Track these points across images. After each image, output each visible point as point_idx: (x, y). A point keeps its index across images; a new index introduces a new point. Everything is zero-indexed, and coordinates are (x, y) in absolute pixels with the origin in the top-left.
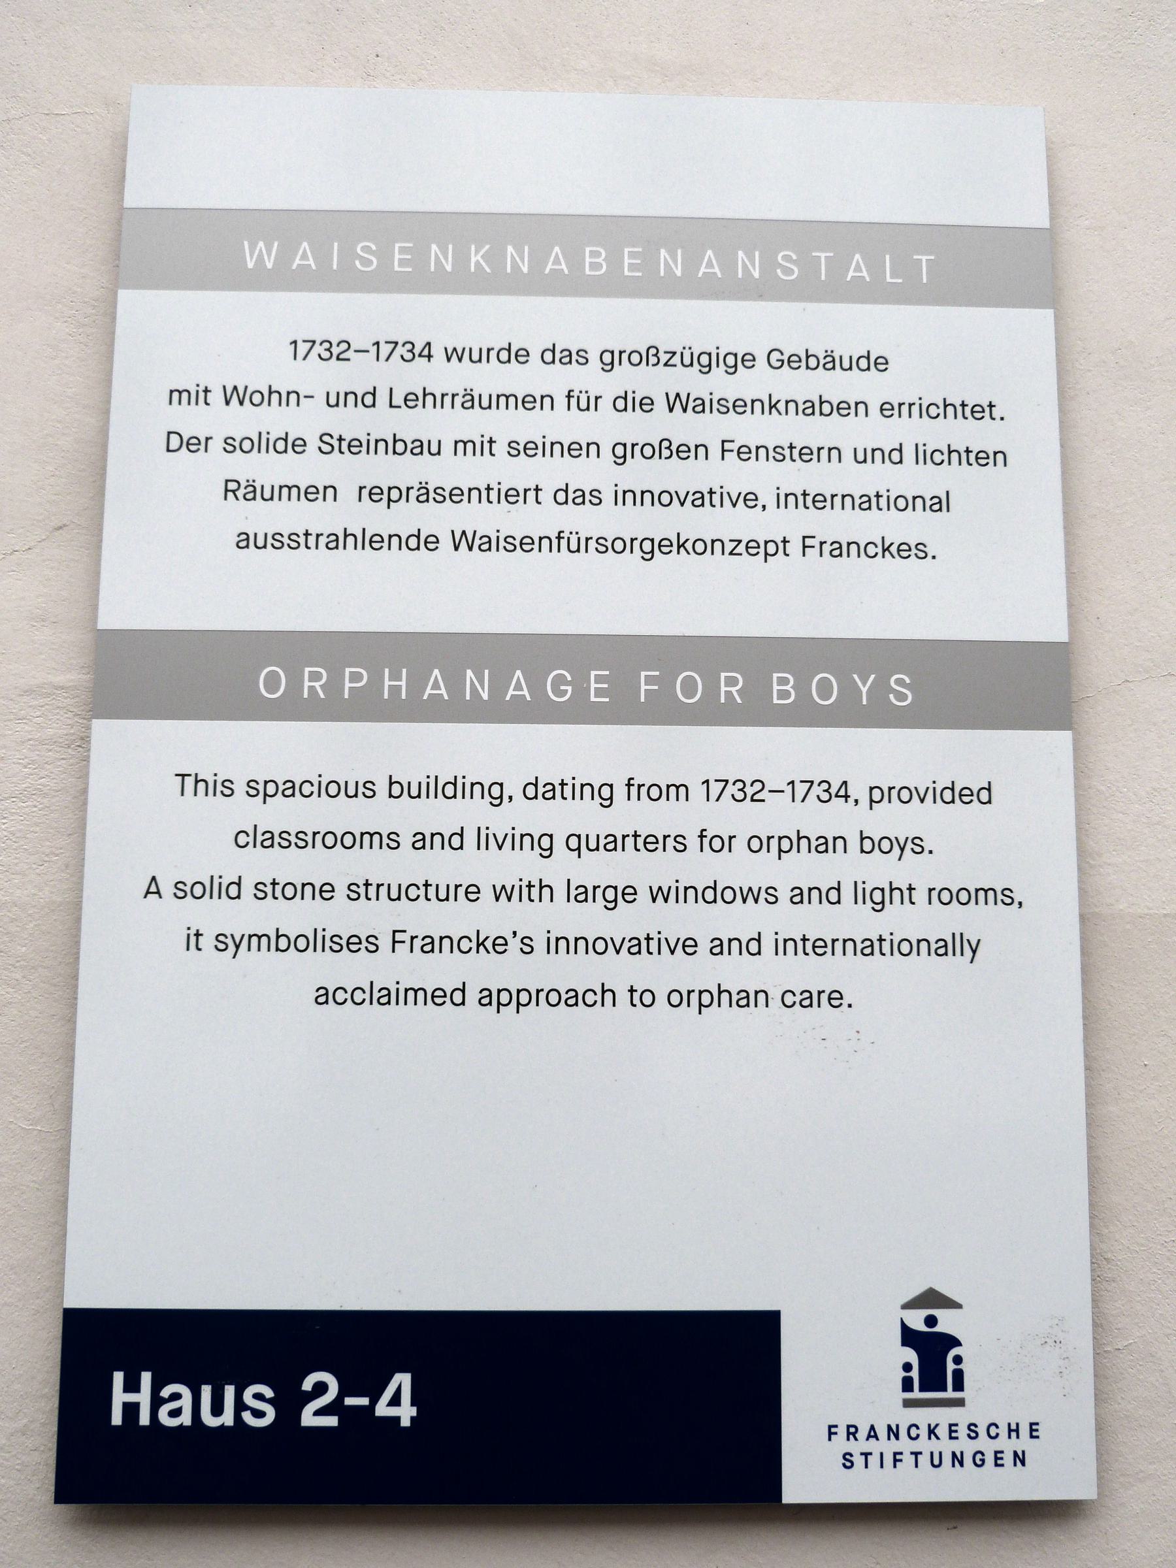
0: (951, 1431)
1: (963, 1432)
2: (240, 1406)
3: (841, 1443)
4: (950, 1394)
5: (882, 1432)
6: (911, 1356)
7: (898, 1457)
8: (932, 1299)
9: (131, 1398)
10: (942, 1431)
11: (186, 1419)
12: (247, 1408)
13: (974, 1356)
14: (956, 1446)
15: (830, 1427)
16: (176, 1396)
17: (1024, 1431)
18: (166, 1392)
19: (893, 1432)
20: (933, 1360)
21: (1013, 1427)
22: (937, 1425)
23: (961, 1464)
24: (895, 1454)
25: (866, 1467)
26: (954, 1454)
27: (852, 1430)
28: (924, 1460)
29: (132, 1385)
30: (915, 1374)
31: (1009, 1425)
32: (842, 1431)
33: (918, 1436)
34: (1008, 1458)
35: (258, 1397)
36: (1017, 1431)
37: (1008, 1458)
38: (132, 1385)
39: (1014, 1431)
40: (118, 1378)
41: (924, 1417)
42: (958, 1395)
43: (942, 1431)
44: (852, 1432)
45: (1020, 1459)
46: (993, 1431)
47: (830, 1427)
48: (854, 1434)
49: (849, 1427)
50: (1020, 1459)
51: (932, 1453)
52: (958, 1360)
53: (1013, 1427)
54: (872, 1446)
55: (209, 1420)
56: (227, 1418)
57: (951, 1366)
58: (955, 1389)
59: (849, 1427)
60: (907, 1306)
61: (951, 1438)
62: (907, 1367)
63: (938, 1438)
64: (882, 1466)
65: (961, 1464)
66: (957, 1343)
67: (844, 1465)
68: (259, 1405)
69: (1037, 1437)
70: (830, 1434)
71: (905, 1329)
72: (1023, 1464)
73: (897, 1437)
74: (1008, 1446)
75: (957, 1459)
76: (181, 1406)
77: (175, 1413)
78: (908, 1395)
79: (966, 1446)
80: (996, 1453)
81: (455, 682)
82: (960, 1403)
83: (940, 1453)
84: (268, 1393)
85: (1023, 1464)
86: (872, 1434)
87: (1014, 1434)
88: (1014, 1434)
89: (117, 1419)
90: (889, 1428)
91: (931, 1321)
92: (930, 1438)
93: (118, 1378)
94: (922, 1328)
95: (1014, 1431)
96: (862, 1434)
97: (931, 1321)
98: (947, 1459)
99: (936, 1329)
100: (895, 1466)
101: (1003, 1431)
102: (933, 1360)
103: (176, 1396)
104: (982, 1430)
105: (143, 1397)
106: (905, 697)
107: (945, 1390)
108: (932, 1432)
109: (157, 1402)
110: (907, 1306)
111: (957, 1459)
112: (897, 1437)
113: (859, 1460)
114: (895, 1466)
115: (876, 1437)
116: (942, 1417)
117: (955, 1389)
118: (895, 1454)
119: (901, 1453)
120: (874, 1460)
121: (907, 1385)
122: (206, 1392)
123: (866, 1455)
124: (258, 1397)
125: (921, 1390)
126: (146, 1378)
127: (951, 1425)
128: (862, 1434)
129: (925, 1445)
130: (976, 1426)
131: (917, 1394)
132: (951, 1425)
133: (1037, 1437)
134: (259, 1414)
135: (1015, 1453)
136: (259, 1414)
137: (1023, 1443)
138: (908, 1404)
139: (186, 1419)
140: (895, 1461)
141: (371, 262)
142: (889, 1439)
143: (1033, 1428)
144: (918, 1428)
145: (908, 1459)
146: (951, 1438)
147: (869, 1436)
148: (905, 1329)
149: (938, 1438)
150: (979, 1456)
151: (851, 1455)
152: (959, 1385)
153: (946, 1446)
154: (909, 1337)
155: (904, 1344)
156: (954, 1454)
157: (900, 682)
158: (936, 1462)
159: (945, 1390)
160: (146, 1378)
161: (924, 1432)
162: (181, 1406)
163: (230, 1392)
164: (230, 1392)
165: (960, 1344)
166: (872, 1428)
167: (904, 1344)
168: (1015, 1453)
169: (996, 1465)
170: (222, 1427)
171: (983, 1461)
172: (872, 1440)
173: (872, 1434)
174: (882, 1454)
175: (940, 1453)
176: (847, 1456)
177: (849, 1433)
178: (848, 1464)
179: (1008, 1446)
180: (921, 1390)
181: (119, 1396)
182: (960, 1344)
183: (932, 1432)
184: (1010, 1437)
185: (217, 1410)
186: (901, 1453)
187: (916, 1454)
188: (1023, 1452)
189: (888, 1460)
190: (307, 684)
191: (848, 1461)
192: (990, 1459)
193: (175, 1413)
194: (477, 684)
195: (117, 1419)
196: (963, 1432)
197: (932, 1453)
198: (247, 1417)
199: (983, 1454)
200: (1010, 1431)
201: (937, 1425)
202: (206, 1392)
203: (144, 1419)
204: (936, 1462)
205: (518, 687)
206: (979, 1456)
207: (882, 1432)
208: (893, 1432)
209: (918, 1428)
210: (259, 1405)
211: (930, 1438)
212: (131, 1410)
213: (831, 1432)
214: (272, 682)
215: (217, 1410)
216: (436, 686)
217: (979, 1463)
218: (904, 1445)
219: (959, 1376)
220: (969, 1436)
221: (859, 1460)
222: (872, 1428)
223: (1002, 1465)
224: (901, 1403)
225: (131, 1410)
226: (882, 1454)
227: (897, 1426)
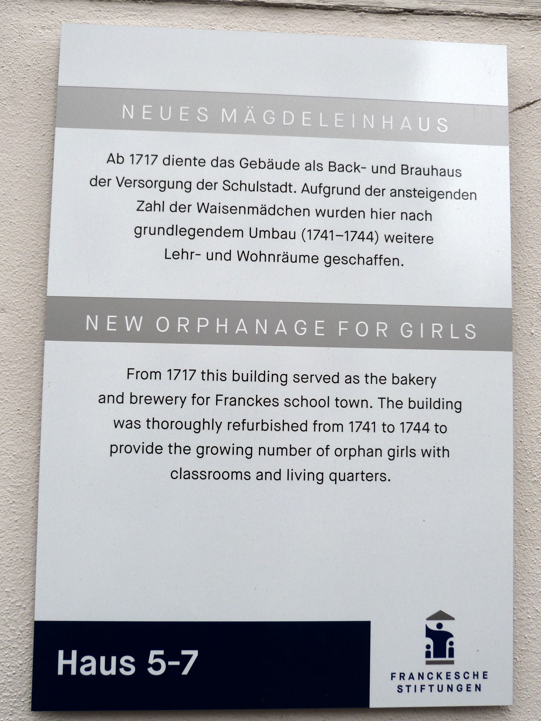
0: (447, 676)
1: (452, 676)
2: (119, 666)
3: (397, 681)
4: (447, 658)
5: (416, 676)
6: (430, 642)
7: (423, 687)
8: (441, 615)
9: (67, 662)
10: (443, 676)
11: (93, 672)
12: (122, 666)
14: (449, 682)
16: (88, 661)
17: (481, 675)
18: (83, 660)
19: (421, 676)
20: (440, 643)
21: (476, 673)
22: (441, 673)
23: (452, 690)
24: (421, 686)
25: (408, 691)
26: (448, 686)
27: (402, 675)
28: (435, 688)
29: (67, 656)
30: (431, 650)
31: (474, 673)
32: (398, 676)
34: (473, 688)
35: (127, 661)
36: (477, 675)
37: (473, 688)
38: (67, 656)
39: (476, 675)
40: (61, 653)
42: (451, 659)
43: (443, 676)
44: (402, 676)
45: (478, 688)
47: (392, 674)
48: (403, 677)
49: (401, 674)
50: (478, 688)
51: (438, 686)
52: (451, 643)
53: (476, 673)
54: (411, 682)
57: (448, 646)
60: (428, 619)
61: (447, 678)
62: (428, 647)
63: (441, 679)
64: (415, 691)
65: (452, 690)
66: (451, 636)
67: (398, 691)
68: (127, 665)
69: (486, 678)
70: (392, 677)
71: (427, 628)
72: (480, 690)
73: (423, 678)
74: (473, 682)
75: (450, 688)
76: (91, 666)
77: (88, 669)
78: (428, 659)
79: (454, 682)
80: (467, 685)
81: (251, 326)
82: (452, 663)
83: (442, 686)
84: (132, 660)
85: (480, 690)
86: (411, 677)
87: (476, 677)
88: (476, 677)
89: (60, 672)
90: (419, 674)
91: (440, 626)
92: (437, 679)
93: (61, 653)
95: (476, 675)
97: (440, 626)
98: (445, 688)
99: (442, 629)
100: (421, 691)
101: (471, 675)
102: (440, 643)
103: (88, 661)
104: (461, 675)
105: (73, 662)
106: (472, 335)
107: (445, 657)
108: (438, 676)
109: (79, 664)
110: (428, 619)
111: (450, 688)
112: (423, 678)
113: (405, 689)
114: (421, 691)
115: (413, 678)
116: (443, 669)
119: (424, 686)
120: (412, 689)
121: (428, 655)
122: (103, 659)
123: (408, 686)
124: (127, 661)
125: (434, 657)
126: (74, 653)
127: (447, 673)
129: (435, 682)
130: (459, 673)
131: (432, 659)
132: (447, 673)
134: (128, 669)
135: (476, 686)
136: (128, 669)
137: (480, 681)
138: (428, 663)
139: (93, 672)
140: (422, 689)
141: (426, 128)
142: (419, 679)
143: (485, 674)
144: (432, 674)
145: (428, 688)
146: (447, 678)
147: (410, 678)
148: (427, 628)
149: (441, 679)
150: (460, 687)
151: (401, 686)
152: (451, 655)
153: (445, 682)
154: (429, 633)
155: (427, 636)
156: (448, 686)
157: (470, 328)
158: (440, 689)
159: (445, 657)
160: (74, 653)
161: (435, 676)
162: (91, 666)
163: (114, 659)
164: (114, 659)
166: (411, 674)
167: (427, 636)
168: (476, 686)
169: (467, 690)
170: (110, 675)
171: (461, 689)
172: (411, 680)
173: (411, 677)
174: (415, 686)
175: (442, 686)
177: (401, 676)
178: (400, 690)
179: (473, 682)
180: (434, 657)
181: (61, 662)
182: (451, 636)
183: (438, 676)
184: (474, 678)
185: (108, 667)
186: (424, 686)
187: (431, 686)
188: (480, 685)
189: (418, 689)
190: (179, 325)
191: (400, 689)
192: (464, 688)
193: (88, 669)
194: (261, 326)
195: (60, 672)
196: (452, 676)
197: (438, 686)
198: (122, 671)
199: (461, 686)
200: (474, 675)
201: (441, 673)
202: (103, 659)
203: (74, 672)
204: (440, 689)
205: (281, 328)
206: (460, 687)
207: (416, 676)
208: (421, 676)
209: (432, 674)
210: (127, 665)
211: (437, 679)
212: (67, 668)
213: (393, 676)
214: (163, 324)
215: (108, 667)
216: (242, 327)
217: (459, 689)
218: (426, 682)
219: (452, 651)
220: (455, 678)
221: (405, 689)
222: (411, 674)
223: (470, 691)
224: (425, 662)
225: (67, 668)
226: (415, 686)
227: (423, 673)
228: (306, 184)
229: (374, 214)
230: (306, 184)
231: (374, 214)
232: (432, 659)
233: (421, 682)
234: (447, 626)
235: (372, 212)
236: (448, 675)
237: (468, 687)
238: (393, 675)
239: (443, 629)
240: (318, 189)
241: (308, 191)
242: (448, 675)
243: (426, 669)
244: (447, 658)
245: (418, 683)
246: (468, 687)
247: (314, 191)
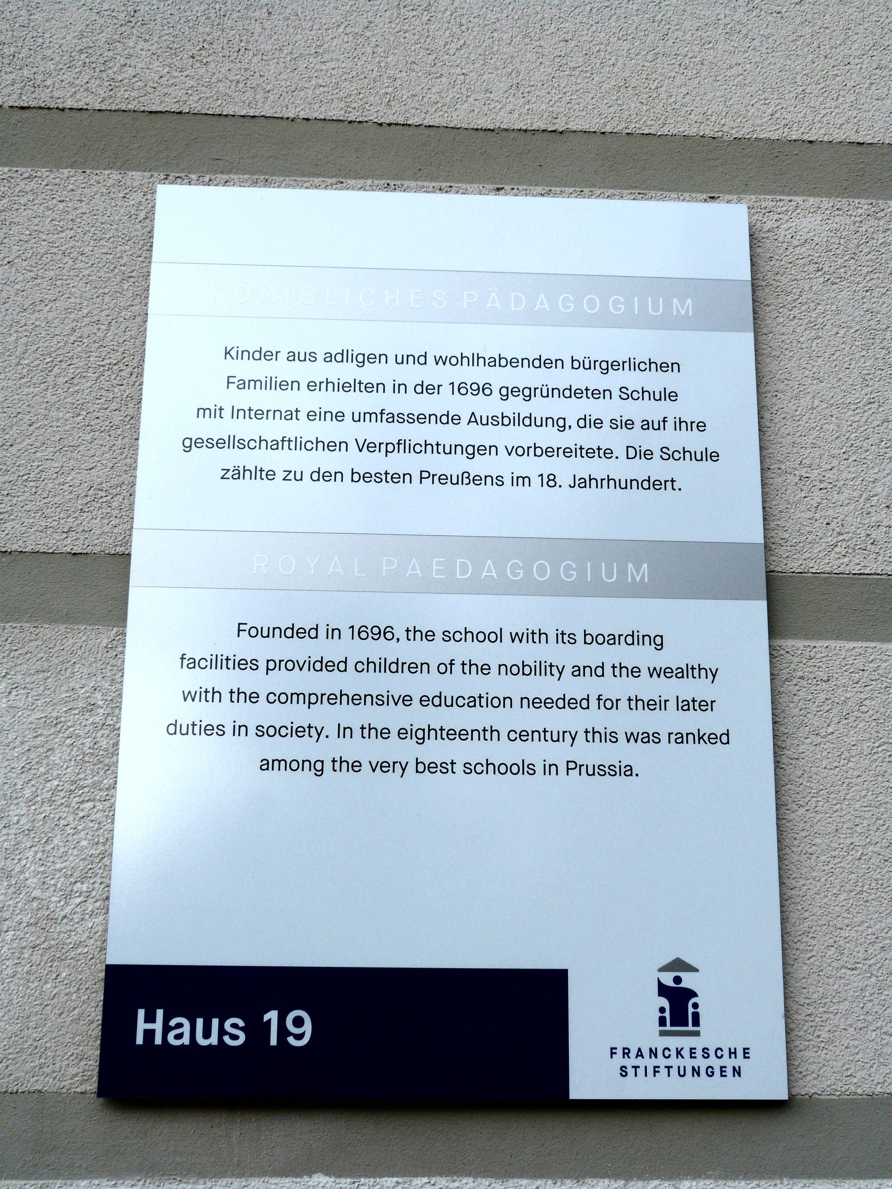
0: (691, 1053)
1: (699, 1053)
2: (222, 1032)
4: (690, 1028)
6: (665, 1003)
10: (686, 1053)
11: (186, 1040)
13: (706, 1004)
16: (180, 1025)
17: (740, 1053)
18: (173, 1023)
19: (653, 1053)
27: (626, 1051)
29: (150, 1018)
30: (667, 1014)
32: (620, 1052)
33: (670, 1055)
34: (729, 1072)
35: (234, 1026)
36: (735, 1053)
37: (729, 1072)
38: (150, 1018)
39: (733, 1053)
40: (141, 1013)
41: (674, 1042)
43: (686, 1053)
46: (719, 1053)
48: (627, 1054)
49: (624, 1049)
50: (737, 1072)
52: (696, 1006)
54: (639, 1062)
55: (201, 1041)
56: (214, 1040)
57: (691, 1010)
58: (694, 1025)
59: (624, 1049)
62: (662, 1010)
66: (695, 995)
67: (621, 1074)
68: (234, 1032)
70: (612, 1053)
71: (660, 984)
75: (696, 1071)
76: (183, 1032)
77: (179, 1037)
79: (701, 1062)
82: (697, 1034)
84: (241, 1023)
85: (739, 1075)
89: (140, 1040)
90: (651, 1049)
91: (678, 980)
93: (141, 1013)
95: (733, 1053)
96: (633, 1054)
97: (678, 980)
98: (689, 1071)
101: (726, 1053)
103: (180, 1025)
104: (712, 1053)
105: (158, 1026)
107: (687, 1026)
108: (679, 1053)
109: (167, 1029)
111: (696, 1071)
113: (631, 1071)
116: (686, 1043)
117: (694, 1025)
121: (662, 1021)
122: (200, 1022)
123: (636, 1068)
124: (234, 1026)
128: (633, 1054)
129: (674, 1061)
131: (668, 1028)
133: (749, 1058)
134: (234, 1037)
135: (734, 1068)
136: (234, 1037)
137: (739, 1061)
138: (663, 1034)
139: (186, 1040)
140: (655, 1072)
147: (637, 1056)
152: (696, 1023)
153: (688, 1063)
154: (663, 990)
155: (660, 994)
158: (682, 1073)
159: (687, 1026)
160: (160, 1013)
161: (673, 1053)
162: (183, 1032)
163: (215, 1022)
164: (215, 1022)
165: (696, 995)
166: (639, 1050)
167: (660, 994)
171: (713, 1073)
173: (640, 1054)
176: (623, 1068)
177: (624, 1053)
179: (729, 1063)
181: (142, 1026)
182: (695, 995)
183: (679, 1053)
185: (207, 1034)
187: (669, 1068)
188: (739, 1067)
193: (179, 1037)
195: (140, 1040)
196: (699, 1053)
198: (226, 1039)
200: (730, 1053)
202: (200, 1022)
203: (158, 1040)
204: (682, 1073)
206: (710, 1070)
208: (653, 1053)
210: (234, 1032)
212: (149, 1035)
215: (207, 1034)
219: (696, 1016)
221: (631, 1071)
222: (639, 1050)
225: (149, 1035)
234: (688, 981)
245: (650, 1063)
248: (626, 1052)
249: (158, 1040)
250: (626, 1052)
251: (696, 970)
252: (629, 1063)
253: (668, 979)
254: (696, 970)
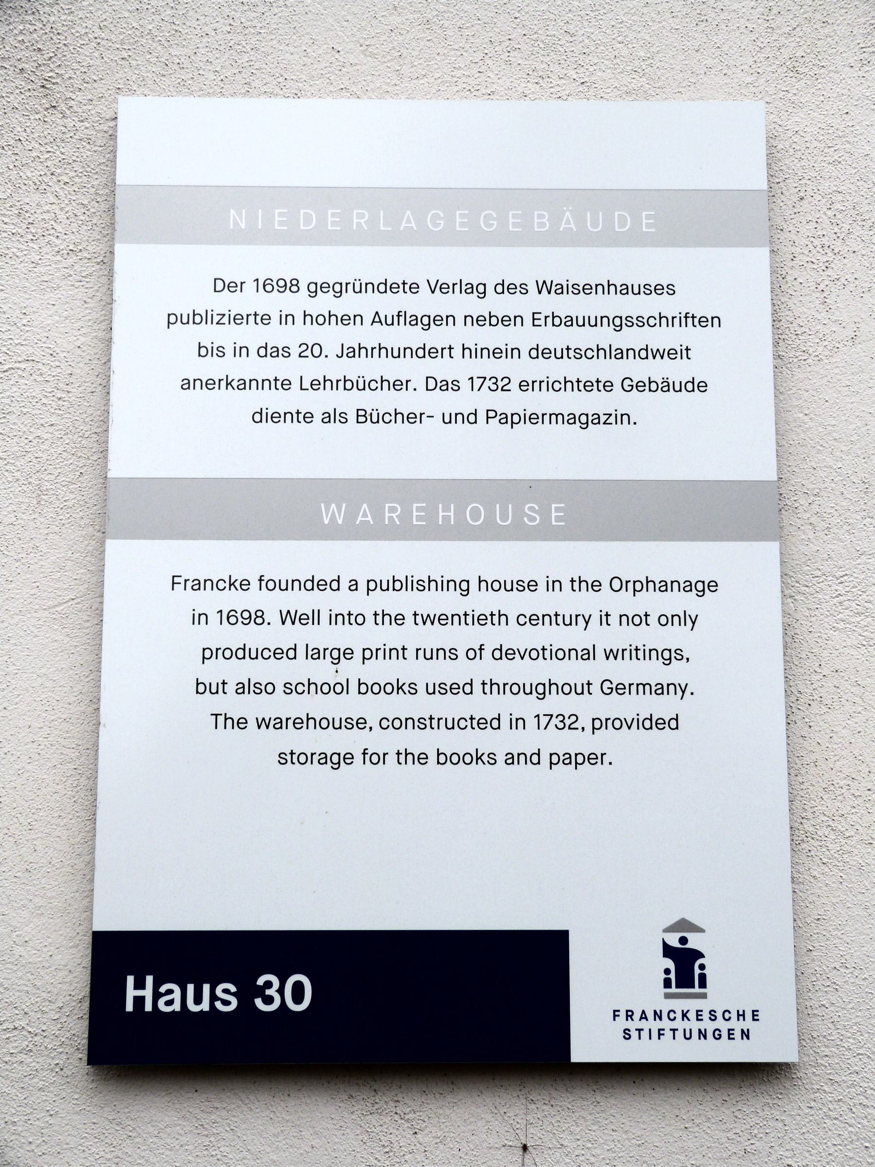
0: (698, 1015)
1: (706, 1015)
2: (213, 998)
3: (622, 1023)
5: (650, 1015)
6: (670, 964)
7: (661, 1032)
9: (140, 993)
10: (692, 1015)
11: (177, 1007)
12: (218, 999)
13: (713, 965)
14: (702, 1025)
15: (615, 1011)
16: (170, 992)
17: (749, 1016)
18: (163, 989)
19: (658, 1015)
20: (685, 966)
23: (705, 1038)
24: (659, 1030)
27: (630, 1013)
28: (679, 1034)
29: (140, 984)
30: (672, 976)
32: (623, 1014)
34: (737, 1034)
35: (226, 991)
36: (743, 1015)
37: (737, 1034)
38: (140, 984)
39: (741, 1015)
40: (130, 980)
41: (679, 1005)
42: (702, 990)
43: (692, 1015)
45: (746, 1034)
47: (615, 1011)
48: (631, 1016)
49: (627, 1011)
50: (746, 1034)
51: (685, 1030)
52: (702, 967)
54: (643, 1024)
55: (192, 1007)
56: (205, 1006)
57: (697, 971)
58: (700, 987)
59: (627, 1011)
62: (667, 971)
65: (705, 1038)
66: (701, 955)
67: (624, 1037)
68: (226, 997)
70: (615, 1016)
71: (666, 946)
72: (748, 1038)
73: (660, 1019)
75: (703, 1034)
76: (174, 998)
77: (169, 1003)
78: (668, 990)
79: (708, 1025)
82: (704, 996)
85: (748, 1038)
86: (644, 1016)
87: (741, 1018)
88: (741, 1018)
90: (655, 1012)
91: (683, 940)
93: (130, 980)
94: (676, 944)
95: (741, 1015)
96: (637, 1016)
97: (683, 940)
98: (695, 1034)
101: (734, 1015)
102: (685, 966)
103: (170, 992)
104: (719, 1015)
105: (148, 993)
107: (694, 987)
108: (684, 1015)
109: (157, 996)
111: (703, 1034)
112: (660, 1019)
113: (634, 1034)
116: (692, 1005)
117: (700, 987)
118: (659, 1030)
120: (645, 1034)
121: (667, 983)
122: (191, 988)
123: (640, 1030)
124: (226, 991)
125: (677, 987)
126: (149, 980)
127: (697, 1011)
128: (637, 1016)
129: (679, 1024)
130: (715, 1012)
132: (697, 1011)
134: (226, 1003)
135: (742, 1031)
136: (226, 1003)
137: (748, 1024)
138: (667, 996)
139: (177, 1007)
140: (660, 1035)
143: (755, 1015)
145: (668, 1034)
148: (666, 946)
150: (717, 1032)
152: (703, 984)
153: (694, 1025)
154: (668, 951)
155: (665, 956)
156: (700, 1031)
158: (688, 1036)
159: (694, 987)
160: (149, 980)
161: (679, 1015)
162: (174, 998)
163: (206, 988)
164: (206, 988)
166: (643, 1012)
167: (665, 955)
168: (742, 1031)
171: (720, 1035)
173: (644, 1016)
176: (626, 1031)
177: (627, 1016)
179: (738, 1026)
180: (677, 987)
181: (131, 993)
182: (702, 956)
183: (684, 1015)
185: (198, 1000)
187: (674, 1030)
188: (748, 1030)
189: (655, 1034)
192: (725, 1034)
193: (169, 1003)
196: (706, 1015)
197: (685, 1030)
198: (218, 1005)
200: (739, 1015)
202: (191, 988)
203: (148, 1007)
204: (688, 1036)
206: (717, 1032)
207: (650, 1015)
208: (658, 1015)
209: (675, 1013)
210: (226, 997)
212: (139, 1001)
213: (615, 1014)
215: (198, 1000)
219: (703, 977)
221: (634, 1034)
222: (643, 1012)
225: (139, 1001)
228: (377, 313)
229: (467, 352)
230: (377, 313)
231: (467, 352)
232: (674, 990)
233: (658, 1024)
234: (694, 942)
235: (464, 349)
236: (699, 1013)
237: (730, 1032)
238: (617, 1013)
239: (689, 946)
240: (396, 318)
241: (380, 322)
242: (699, 1013)
243: (665, 1006)
244: (697, 990)
246: (730, 1032)
247: (389, 321)
248: (630, 1015)
249: (148, 1007)
250: (630, 1015)
251: (702, 931)
252: (633, 1025)
253: (673, 940)
254: (702, 931)
